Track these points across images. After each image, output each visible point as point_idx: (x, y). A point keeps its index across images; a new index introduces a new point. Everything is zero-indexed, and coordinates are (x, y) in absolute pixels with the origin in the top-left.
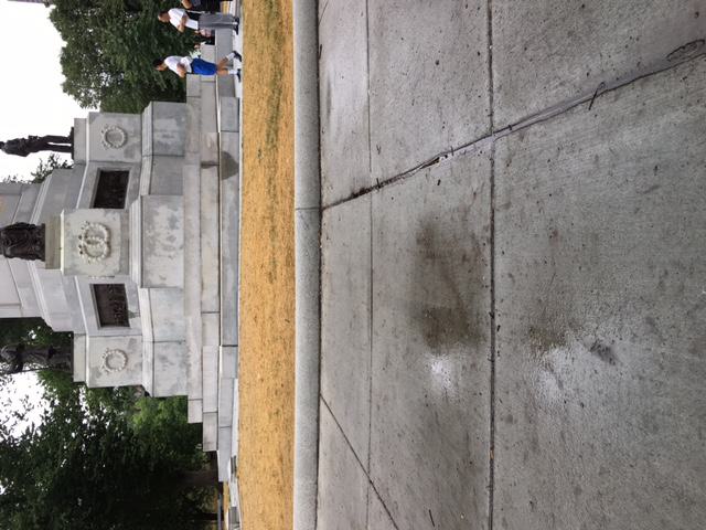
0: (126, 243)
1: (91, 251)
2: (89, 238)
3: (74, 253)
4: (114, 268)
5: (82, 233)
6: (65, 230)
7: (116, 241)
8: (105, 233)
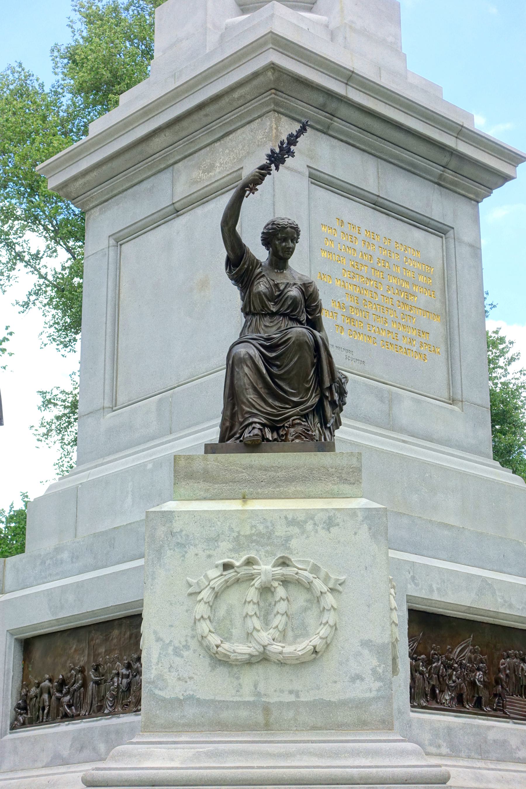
0: (266, 720)
1: (233, 597)
2: (281, 592)
3: (225, 545)
4: (171, 678)
5: (300, 569)
6: (310, 515)
7: (274, 686)
8: (301, 647)
